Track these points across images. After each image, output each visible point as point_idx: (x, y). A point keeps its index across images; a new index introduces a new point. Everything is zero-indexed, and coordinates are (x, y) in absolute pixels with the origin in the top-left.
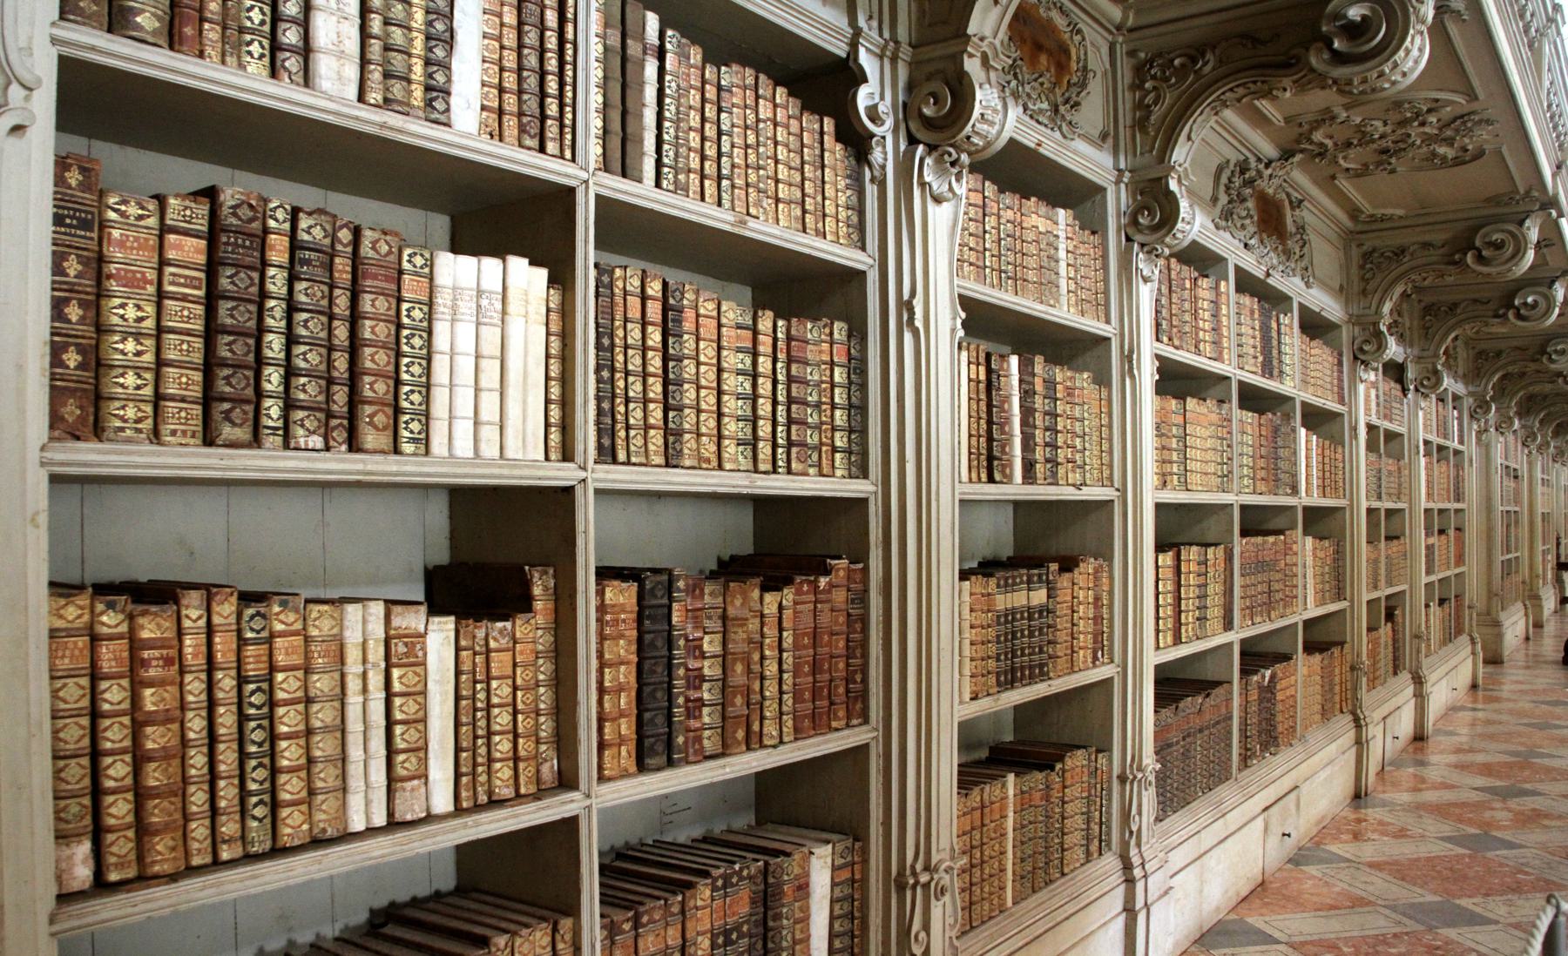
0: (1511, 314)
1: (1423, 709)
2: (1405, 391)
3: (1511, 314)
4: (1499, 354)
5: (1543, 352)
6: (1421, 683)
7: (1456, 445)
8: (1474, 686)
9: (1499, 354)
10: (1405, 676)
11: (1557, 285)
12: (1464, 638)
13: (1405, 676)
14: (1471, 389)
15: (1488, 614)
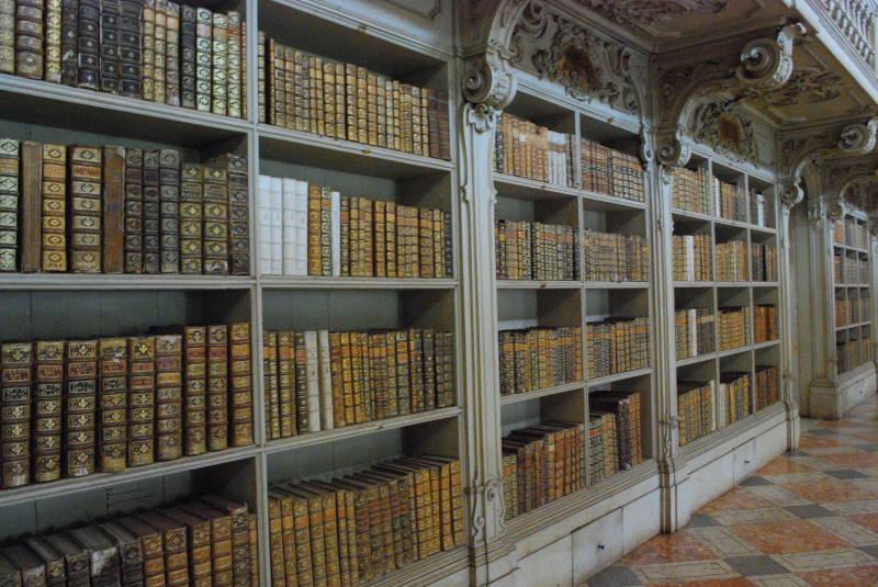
0: (739, 74)
1: (668, 500)
2: (643, 163)
3: (739, 74)
4: (802, 142)
5: (839, 139)
6: (667, 473)
7: (761, 226)
8: (789, 450)
9: (802, 142)
10: (652, 464)
11: (782, 36)
12: (780, 405)
13: (652, 464)
14: (780, 176)
15: (825, 377)
